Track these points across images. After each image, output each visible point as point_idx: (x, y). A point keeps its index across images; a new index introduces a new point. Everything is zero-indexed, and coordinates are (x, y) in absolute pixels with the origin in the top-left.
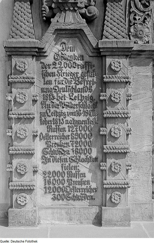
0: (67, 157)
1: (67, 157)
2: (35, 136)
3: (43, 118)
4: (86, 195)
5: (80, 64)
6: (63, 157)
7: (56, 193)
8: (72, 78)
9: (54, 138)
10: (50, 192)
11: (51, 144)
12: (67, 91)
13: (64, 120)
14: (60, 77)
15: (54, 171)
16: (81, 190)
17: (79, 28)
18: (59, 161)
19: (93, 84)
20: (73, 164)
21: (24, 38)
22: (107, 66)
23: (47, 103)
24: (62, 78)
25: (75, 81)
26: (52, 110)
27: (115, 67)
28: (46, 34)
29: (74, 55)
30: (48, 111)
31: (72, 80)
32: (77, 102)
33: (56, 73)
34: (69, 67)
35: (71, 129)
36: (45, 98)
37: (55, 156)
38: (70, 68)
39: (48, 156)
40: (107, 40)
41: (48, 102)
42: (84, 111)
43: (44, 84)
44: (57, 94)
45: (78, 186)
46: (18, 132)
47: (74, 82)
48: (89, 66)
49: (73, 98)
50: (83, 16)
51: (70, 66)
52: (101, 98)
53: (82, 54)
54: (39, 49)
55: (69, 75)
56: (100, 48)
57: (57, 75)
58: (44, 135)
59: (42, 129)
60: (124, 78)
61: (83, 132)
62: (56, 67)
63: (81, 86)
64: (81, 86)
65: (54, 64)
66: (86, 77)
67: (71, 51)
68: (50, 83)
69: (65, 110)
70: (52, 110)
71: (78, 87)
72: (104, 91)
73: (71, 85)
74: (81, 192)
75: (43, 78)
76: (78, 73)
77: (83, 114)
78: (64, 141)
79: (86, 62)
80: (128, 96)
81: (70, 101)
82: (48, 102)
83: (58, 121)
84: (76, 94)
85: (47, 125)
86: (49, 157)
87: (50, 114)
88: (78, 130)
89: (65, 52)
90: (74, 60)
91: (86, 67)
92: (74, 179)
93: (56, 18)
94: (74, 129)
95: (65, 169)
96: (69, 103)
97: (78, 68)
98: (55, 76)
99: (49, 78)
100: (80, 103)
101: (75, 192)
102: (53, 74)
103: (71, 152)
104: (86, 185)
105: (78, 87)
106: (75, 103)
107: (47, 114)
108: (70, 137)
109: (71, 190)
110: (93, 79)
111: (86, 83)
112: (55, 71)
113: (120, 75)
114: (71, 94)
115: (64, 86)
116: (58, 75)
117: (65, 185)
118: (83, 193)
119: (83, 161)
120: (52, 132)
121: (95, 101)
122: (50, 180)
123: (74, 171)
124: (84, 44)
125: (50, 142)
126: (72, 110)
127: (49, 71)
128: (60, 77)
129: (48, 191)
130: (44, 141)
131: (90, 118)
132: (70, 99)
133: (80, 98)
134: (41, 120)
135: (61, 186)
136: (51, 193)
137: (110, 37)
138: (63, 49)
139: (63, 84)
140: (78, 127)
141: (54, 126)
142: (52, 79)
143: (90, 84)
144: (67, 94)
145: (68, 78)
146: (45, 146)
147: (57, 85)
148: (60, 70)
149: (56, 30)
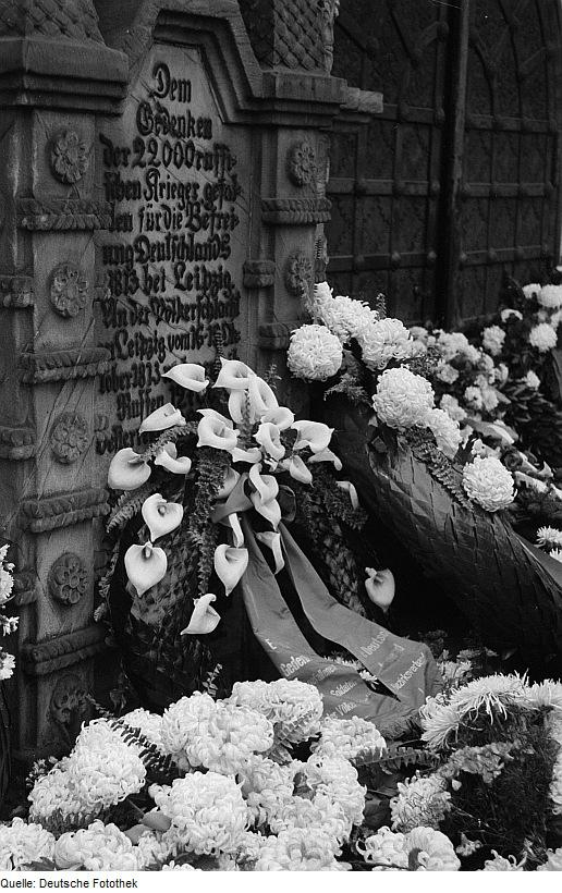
14: (152, 201)
25: (191, 219)
33: (144, 186)
34: (175, 163)
48: (223, 164)
49: (183, 281)
51: (178, 157)
53: (205, 116)
57: (145, 193)
63: (202, 237)
64: (202, 237)
65: (138, 143)
67: (180, 100)
68: (124, 223)
69: (166, 330)
77: (206, 341)
79: (216, 146)
81: (178, 292)
84: (190, 267)
85: (120, 391)
96: (173, 301)
107: (120, 349)
112: (138, 174)
114: (179, 267)
124: (218, 75)
126: (183, 328)
128: (152, 201)
132: (178, 286)
139: (158, 229)
141: (134, 395)
144: (167, 265)
145: (172, 203)
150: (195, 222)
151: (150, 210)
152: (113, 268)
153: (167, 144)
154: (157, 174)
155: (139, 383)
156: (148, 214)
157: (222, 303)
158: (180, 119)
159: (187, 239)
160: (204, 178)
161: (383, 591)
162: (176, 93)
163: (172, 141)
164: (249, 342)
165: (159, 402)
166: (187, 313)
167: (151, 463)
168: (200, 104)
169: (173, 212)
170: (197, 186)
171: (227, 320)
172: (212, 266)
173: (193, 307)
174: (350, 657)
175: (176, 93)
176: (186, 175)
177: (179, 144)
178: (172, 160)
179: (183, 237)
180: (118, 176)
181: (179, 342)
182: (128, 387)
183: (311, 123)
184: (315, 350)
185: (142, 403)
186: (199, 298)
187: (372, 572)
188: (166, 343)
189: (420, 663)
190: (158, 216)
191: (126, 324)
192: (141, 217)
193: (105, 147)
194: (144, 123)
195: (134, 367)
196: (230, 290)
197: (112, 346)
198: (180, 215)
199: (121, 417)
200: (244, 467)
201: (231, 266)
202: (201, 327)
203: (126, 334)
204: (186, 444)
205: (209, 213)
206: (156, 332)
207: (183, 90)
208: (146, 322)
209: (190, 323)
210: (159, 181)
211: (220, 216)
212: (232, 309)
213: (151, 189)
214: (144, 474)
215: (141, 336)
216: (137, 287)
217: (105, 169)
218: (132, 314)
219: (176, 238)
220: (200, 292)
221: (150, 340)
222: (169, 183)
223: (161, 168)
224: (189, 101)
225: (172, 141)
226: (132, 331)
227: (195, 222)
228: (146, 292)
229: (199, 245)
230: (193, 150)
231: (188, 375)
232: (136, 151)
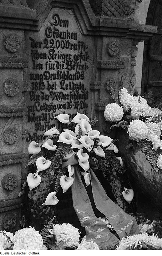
8: (64, 61)
12: (58, 79)
14: (51, 60)
23: (36, 94)
24: (53, 62)
25: (68, 66)
29: (68, 31)
30: (37, 105)
31: (65, 64)
33: (48, 54)
34: (61, 47)
38: (63, 48)
42: (75, 103)
43: (34, 69)
44: (48, 82)
47: (65, 66)
48: (82, 48)
49: (64, 87)
51: (63, 45)
55: (61, 57)
57: (48, 57)
63: (72, 72)
64: (72, 72)
65: (46, 41)
67: (64, 27)
68: (40, 67)
69: (56, 102)
70: (42, 103)
75: (33, 60)
76: (71, 55)
77: (73, 107)
79: (79, 42)
81: (62, 90)
84: (67, 82)
87: (39, 108)
89: (58, 27)
91: (79, 48)
96: (60, 93)
97: (71, 49)
98: (46, 58)
99: (40, 61)
100: (72, 92)
102: (43, 56)
106: (66, 93)
107: (36, 108)
112: (46, 51)
114: (62, 82)
121: (86, 91)
126: (63, 102)
127: (40, 51)
128: (51, 60)
132: (62, 88)
133: (72, 87)
138: (56, 23)
139: (54, 69)
141: (42, 123)
142: (43, 62)
144: (58, 82)
145: (60, 61)
147: (48, 70)
148: (51, 51)
150: (69, 67)
151: (50, 63)
152: (34, 81)
153: (58, 41)
154: (53, 51)
155: (45, 119)
156: (49, 64)
157: (80, 94)
158: (63, 33)
159: (66, 73)
160: (73, 53)
161: (129, 196)
162: (62, 24)
163: (60, 40)
164: (92, 108)
165: (53, 126)
166: (65, 97)
167: (41, 147)
168: (72, 28)
169: (60, 64)
170: (70, 55)
171: (83, 100)
172: (76, 82)
173: (68, 95)
174: (106, 219)
175: (62, 24)
176: (66, 51)
177: (63, 41)
178: (60, 46)
179: (64, 72)
180: (37, 51)
181: (63, 107)
182: (40, 120)
183: (117, 35)
184: (113, 112)
185: (46, 126)
186: (71, 92)
187: (125, 189)
188: (56, 107)
189: (131, 224)
190: (54, 65)
191: (39, 100)
192: (46, 65)
193: (32, 41)
194: (48, 34)
195: (43, 114)
196: (84, 90)
197: (33, 107)
198: (63, 65)
199: (37, 130)
200: (76, 150)
201: (85, 82)
202: (71, 102)
203: (39, 104)
204: (55, 139)
205: (75, 64)
206: (52, 103)
207: (66, 23)
208: (48, 100)
209: (66, 101)
210: (54, 53)
211: (80, 66)
212: (85, 96)
213: (51, 56)
214: (38, 150)
215: (46, 104)
216: (44, 88)
217: (31, 49)
218: (42, 97)
219: (61, 72)
220: (71, 91)
221: (50, 105)
222: (58, 54)
223: (55, 49)
224: (68, 27)
225: (60, 40)
226: (42, 103)
227: (69, 67)
228: (48, 89)
229: (71, 75)
230: (69, 43)
231: (63, 118)
232: (45, 43)
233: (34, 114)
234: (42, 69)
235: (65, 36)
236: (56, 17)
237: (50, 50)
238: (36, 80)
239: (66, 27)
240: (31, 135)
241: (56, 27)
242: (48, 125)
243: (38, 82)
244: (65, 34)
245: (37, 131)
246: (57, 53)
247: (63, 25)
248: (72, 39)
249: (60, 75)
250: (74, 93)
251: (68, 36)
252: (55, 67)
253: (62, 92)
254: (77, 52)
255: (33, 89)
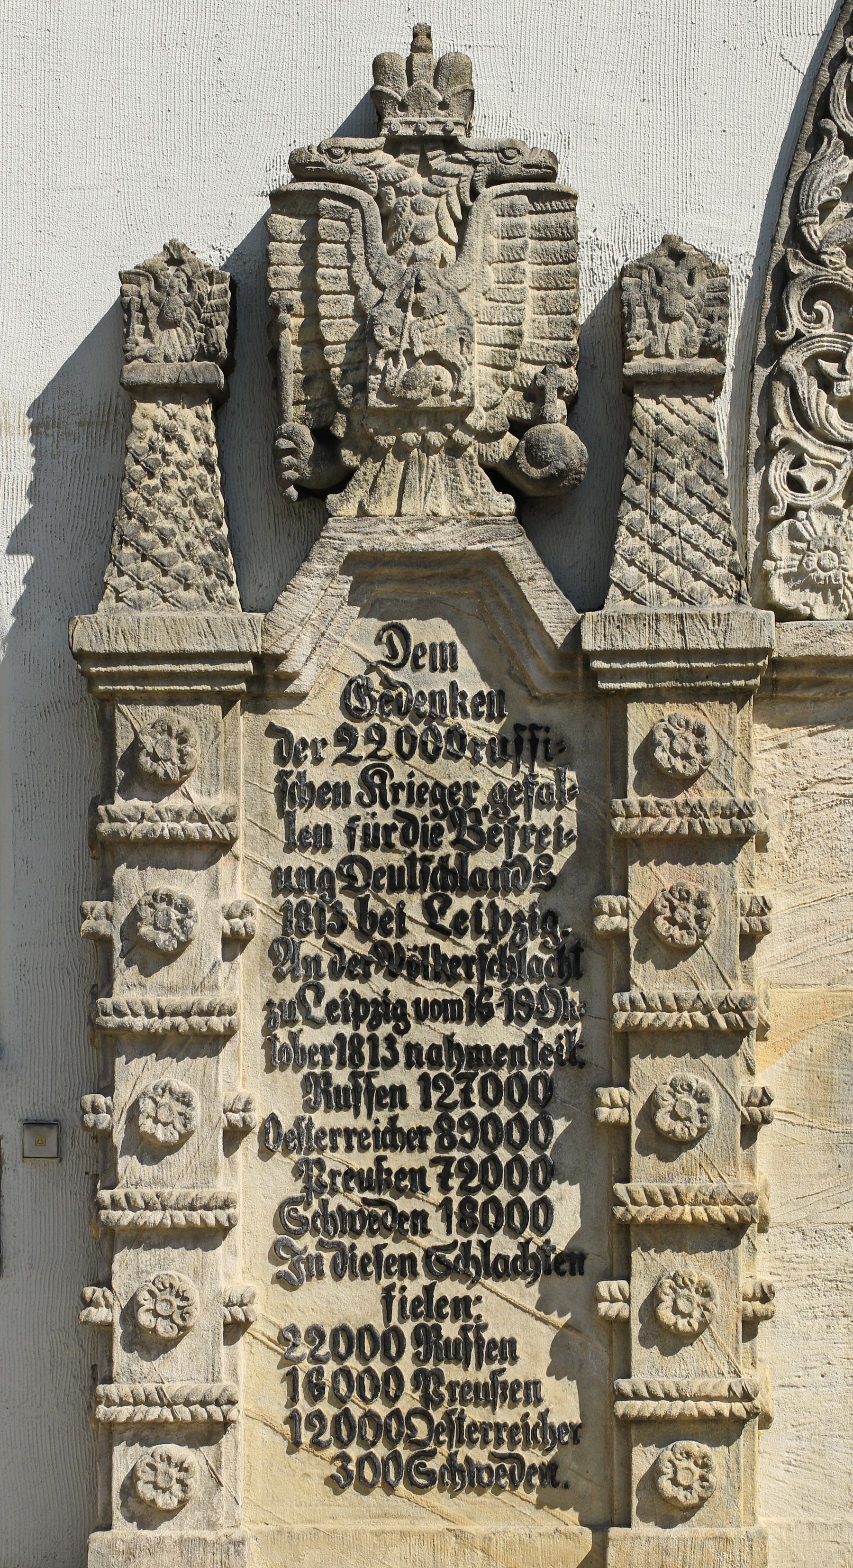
0: (416, 1246)
1: (416, 1246)
2: (233, 1137)
3: (282, 1035)
4: (519, 1459)
5: (487, 737)
6: (395, 1249)
7: (354, 1451)
9: (341, 1142)
10: (317, 1445)
11: (326, 1178)
13: (400, 1047)
15: (344, 1329)
16: (492, 1435)
17: (480, 546)
18: (371, 1268)
19: (558, 847)
20: (450, 1289)
21: (178, 603)
22: (633, 747)
26: (332, 989)
27: (675, 754)
28: (301, 579)
29: (453, 685)
30: (310, 995)
31: (444, 824)
32: (469, 945)
35: (435, 1096)
36: (295, 921)
37: (346, 1241)
39: (307, 1243)
40: (629, 606)
41: (310, 946)
42: (507, 994)
44: (361, 905)
45: (475, 1414)
46: (147, 1106)
47: (449, 836)
50: (501, 477)
52: (603, 923)
54: (258, 659)
56: (589, 656)
58: (287, 1125)
59: (280, 1097)
60: (724, 816)
61: (504, 1113)
62: (355, 753)
63: (485, 860)
65: (345, 736)
66: (520, 811)
67: (433, 669)
69: (401, 989)
70: (332, 989)
71: (473, 862)
72: (614, 883)
73: (438, 854)
74: (491, 1448)
78: (397, 1160)
79: (518, 728)
80: (750, 914)
81: (432, 940)
82: (310, 946)
83: (366, 1049)
84: (463, 903)
86: (312, 1251)
88: (475, 1097)
90: (454, 715)
92: (452, 1372)
93: (357, 492)
94: (455, 1096)
95: (403, 1317)
96: (424, 951)
97: (476, 760)
100: (488, 948)
101: (460, 1442)
103: (435, 1222)
104: (521, 1409)
105: (473, 862)
106: (460, 952)
108: (431, 1140)
109: (434, 1431)
110: (560, 819)
111: (517, 841)
113: (703, 794)
114: (436, 905)
115: (397, 860)
116: (366, 799)
117: (405, 1405)
118: (504, 1450)
119: (502, 1269)
120: (328, 1108)
122: (320, 1372)
123: (450, 1330)
125: (320, 1163)
127: (317, 775)
128: (377, 808)
129: (306, 1437)
130: (282, 1166)
131: (542, 1031)
134: (270, 1041)
135: (380, 1408)
136: (327, 1445)
137: (649, 588)
138: (394, 654)
140: (475, 1085)
143: (540, 846)
146: (295, 1189)
147: (357, 851)
149: (351, 555)
151: (371, 822)
152: (294, 900)
173: (468, 961)
175: (425, 661)
176: (449, 772)
179: (444, 859)
180: (302, 776)
186: (482, 949)
188: (410, 1010)
190: (389, 829)
195: (340, 1038)
199: (310, 1107)
202: (489, 991)
206: (386, 992)
210: (388, 782)
211: (525, 832)
224: (454, 668)
228: (363, 935)
229: (479, 871)
230: (463, 736)
233: (293, 1037)
234: (329, 846)
235: (443, 708)
236: (390, 638)
237: (367, 769)
238: (299, 892)
239: (444, 669)
240: (285, 1129)
241: (392, 675)
242: (370, 1087)
243: (313, 903)
244: (442, 700)
245: (314, 1109)
246: (405, 781)
247: (427, 666)
248: (477, 716)
249: (424, 872)
250: (502, 949)
251: (453, 705)
252: (395, 838)
253: (436, 947)
254: (507, 776)
255: (285, 933)
